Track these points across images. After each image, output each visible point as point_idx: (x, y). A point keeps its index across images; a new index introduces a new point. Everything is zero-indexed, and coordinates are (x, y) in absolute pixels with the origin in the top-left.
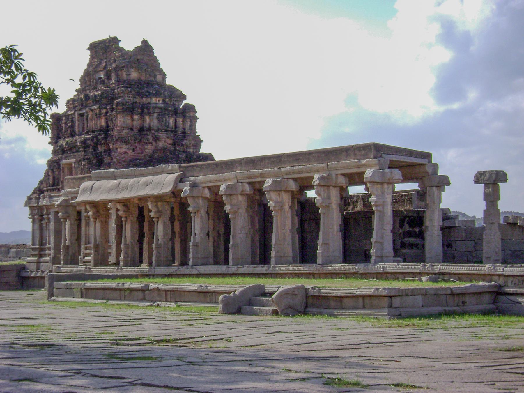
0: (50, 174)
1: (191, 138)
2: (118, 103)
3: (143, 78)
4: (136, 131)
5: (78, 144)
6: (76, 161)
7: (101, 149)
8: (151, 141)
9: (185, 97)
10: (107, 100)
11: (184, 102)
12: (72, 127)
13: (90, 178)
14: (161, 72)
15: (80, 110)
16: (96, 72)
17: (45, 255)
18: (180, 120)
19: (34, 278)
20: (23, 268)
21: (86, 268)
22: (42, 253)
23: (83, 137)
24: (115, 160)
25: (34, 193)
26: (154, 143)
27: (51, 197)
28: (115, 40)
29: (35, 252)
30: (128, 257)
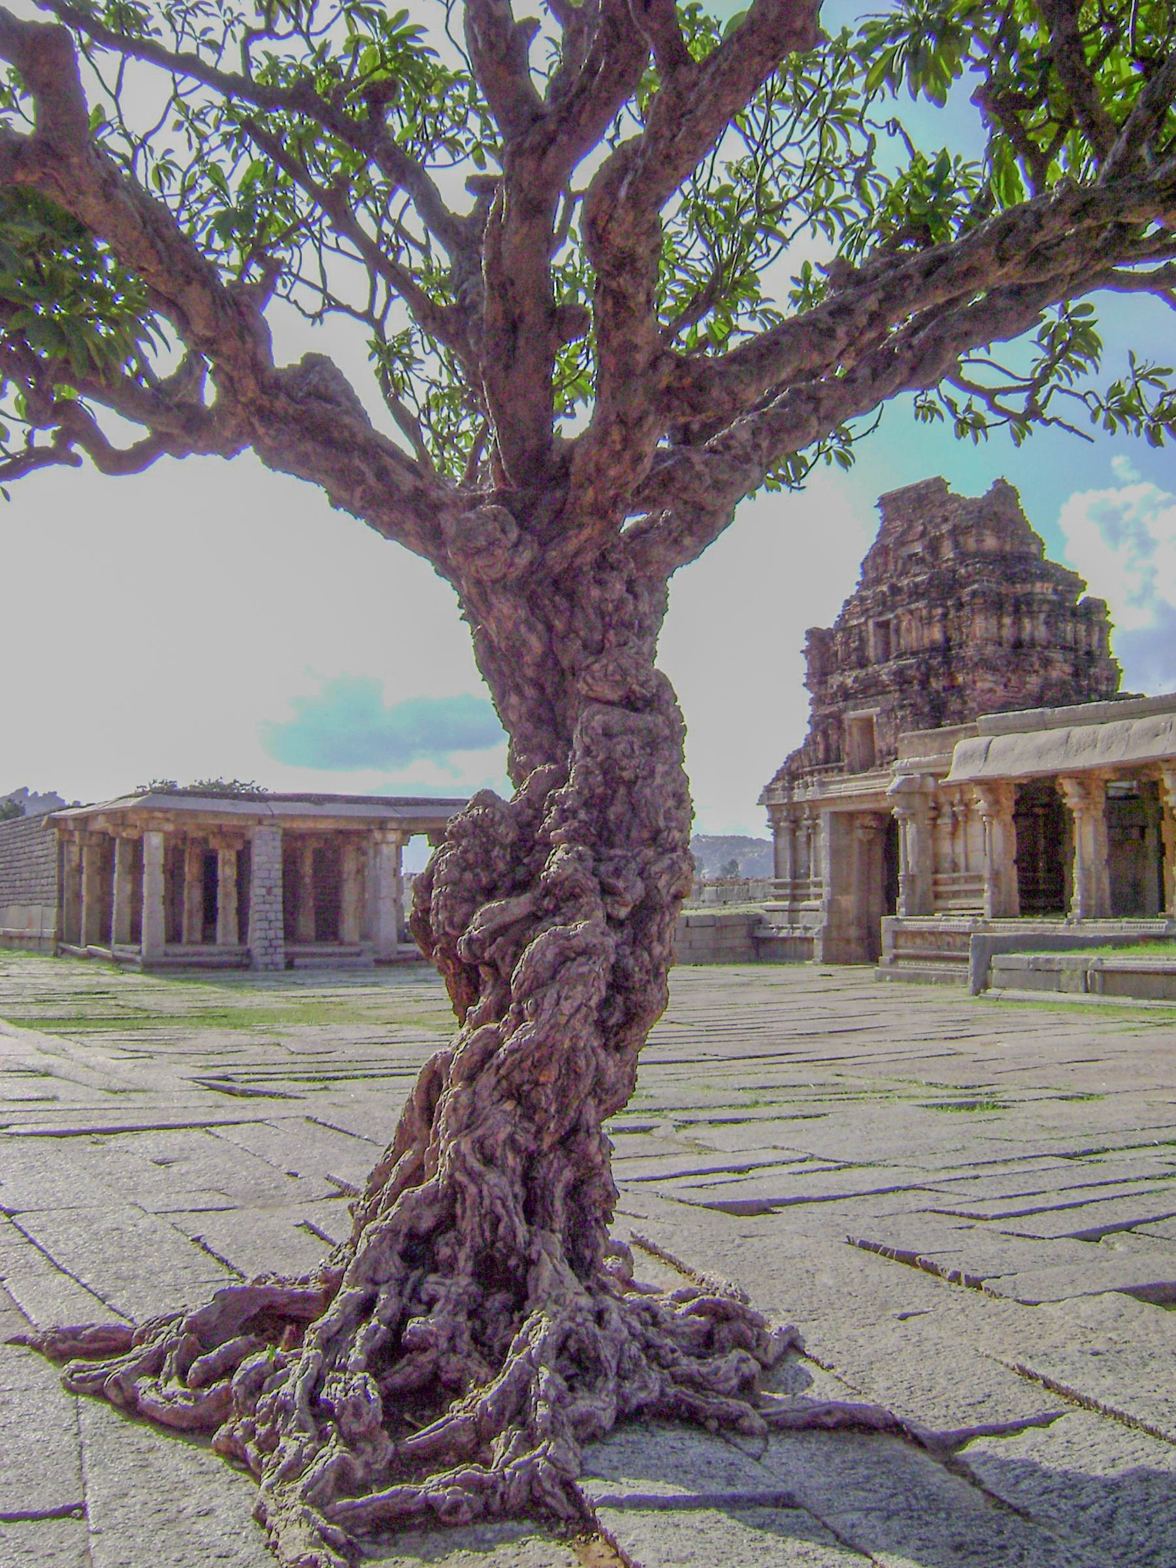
0: (819, 739)
1: (1102, 663)
2: (974, 594)
3: (1008, 548)
4: (1007, 648)
5: (884, 677)
6: (883, 711)
7: (936, 684)
8: (1036, 667)
9: (1082, 585)
10: (944, 589)
11: (1081, 597)
12: (861, 648)
13: (973, 732)
14: (1035, 536)
15: (880, 614)
16: (902, 543)
17: (807, 897)
18: (1082, 628)
19: (784, 939)
20: (758, 921)
21: (976, 922)
22: (799, 892)
23: (892, 665)
24: (973, 705)
25: (777, 779)
26: (1042, 672)
27: (822, 784)
28: (939, 485)
29: (781, 892)
30: (1090, 898)
